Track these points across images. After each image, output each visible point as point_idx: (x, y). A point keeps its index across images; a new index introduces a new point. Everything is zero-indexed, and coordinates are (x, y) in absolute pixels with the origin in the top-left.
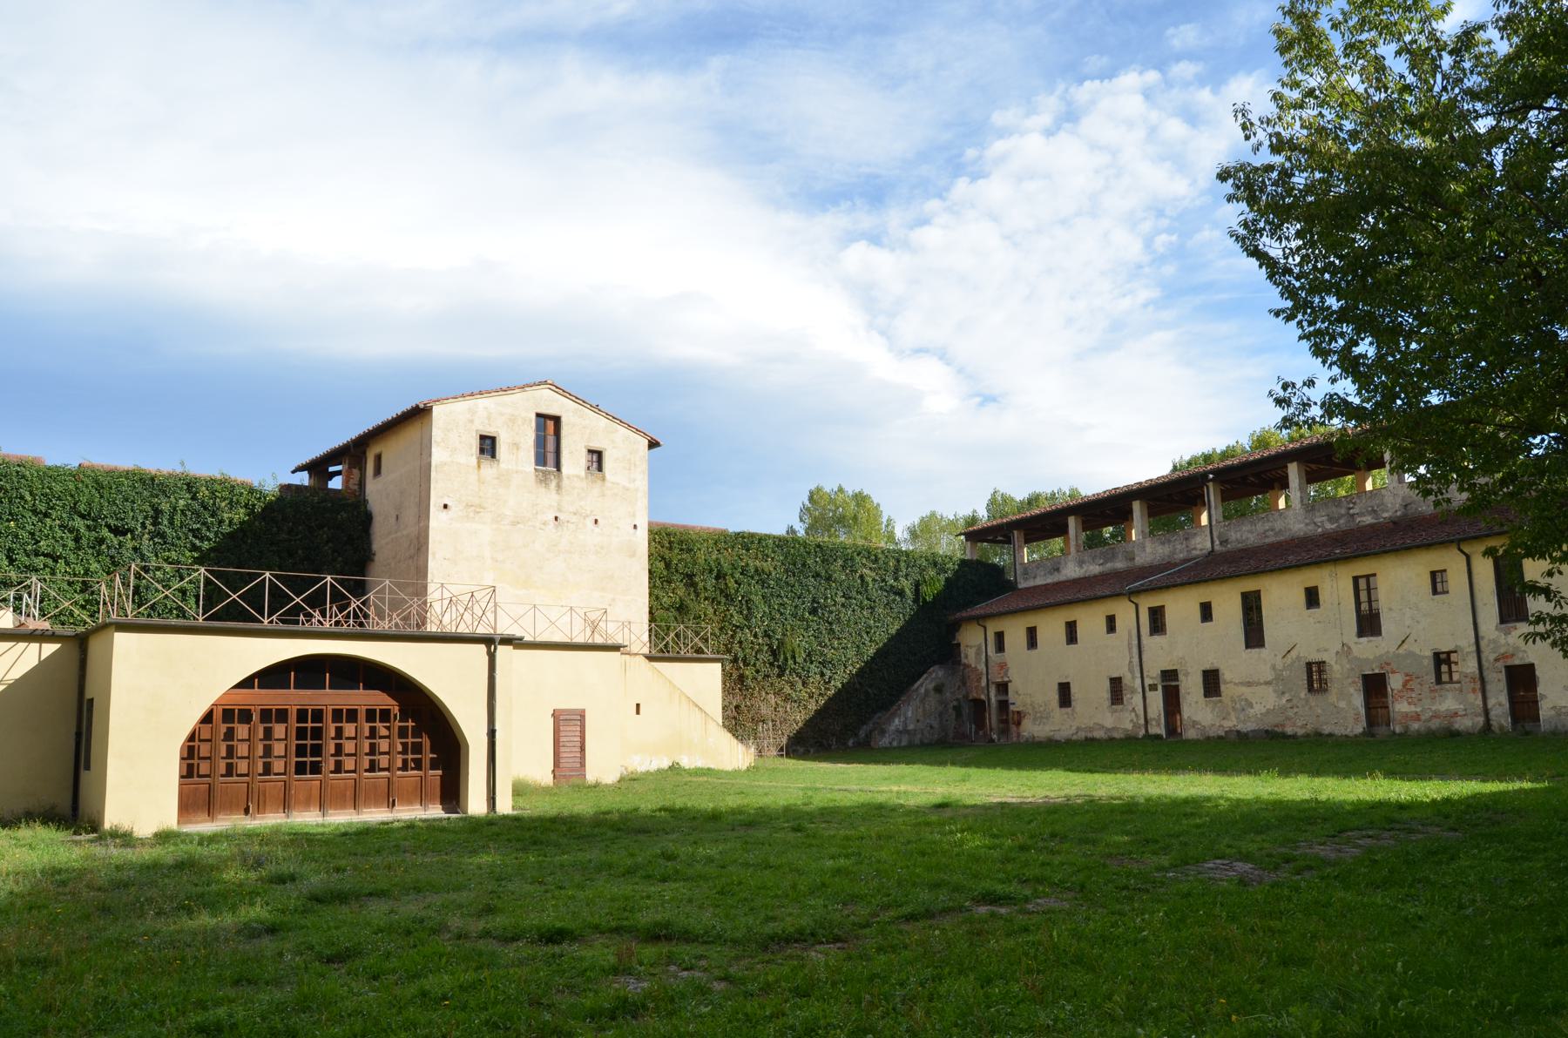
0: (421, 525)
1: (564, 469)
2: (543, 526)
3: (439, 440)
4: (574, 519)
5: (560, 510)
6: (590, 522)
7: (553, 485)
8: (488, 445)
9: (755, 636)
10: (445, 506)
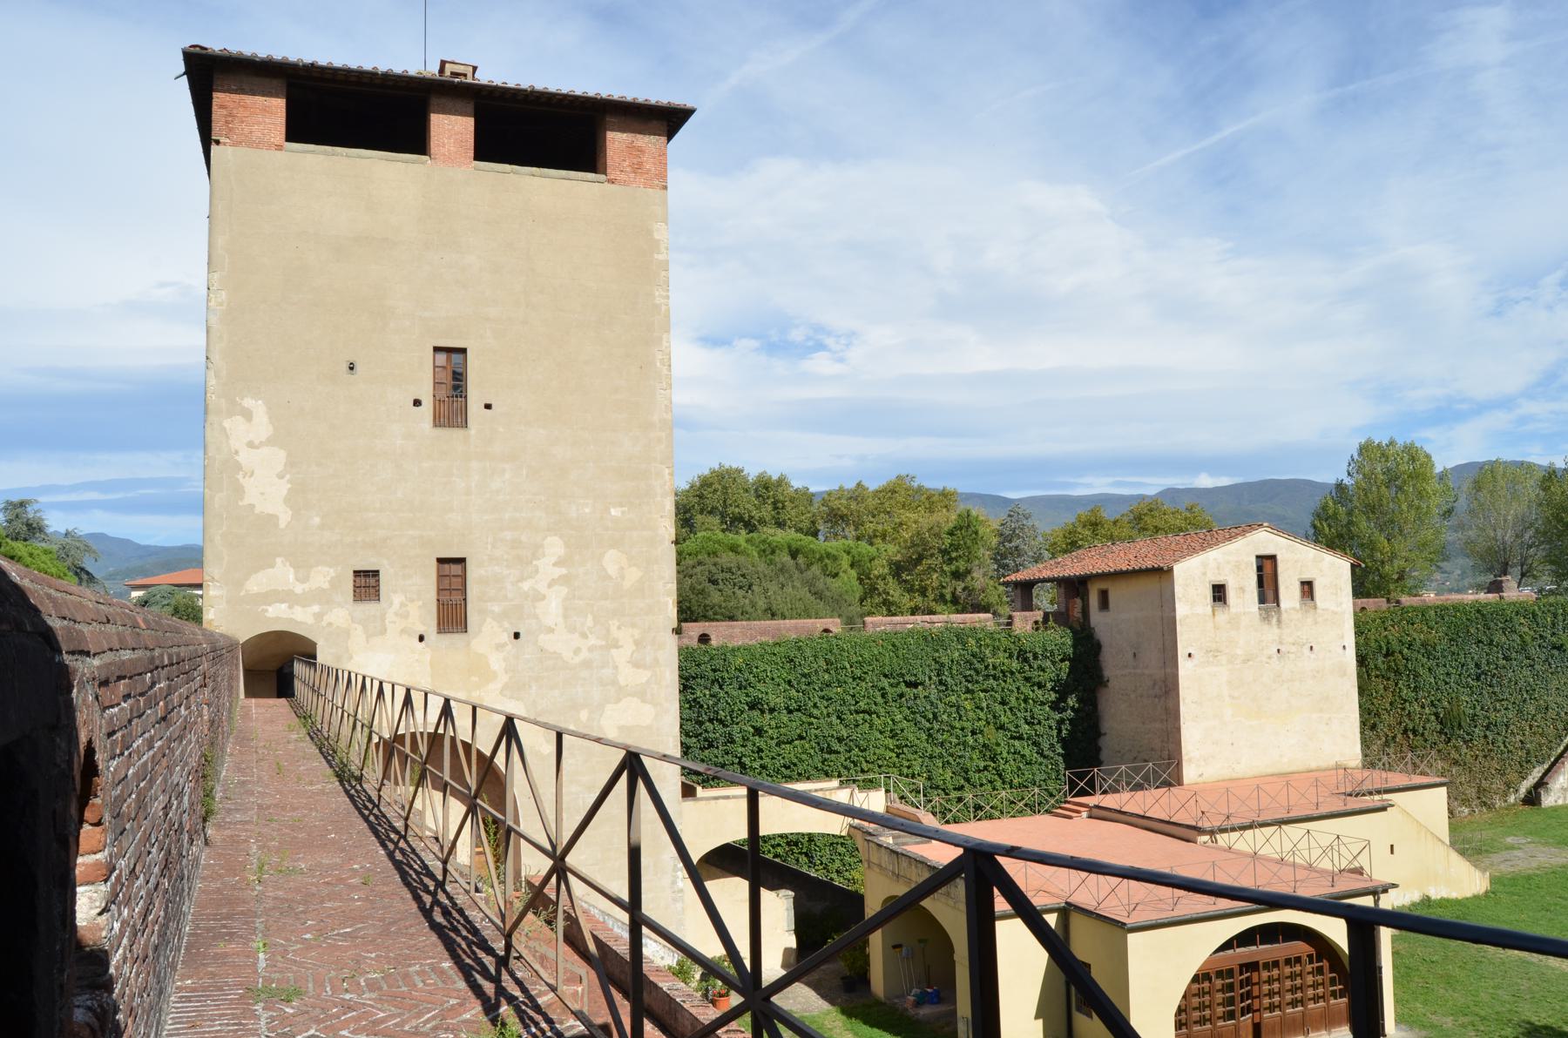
0: (1168, 670)
1: (1283, 605)
2: (1268, 660)
3: (1180, 596)
4: (1293, 649)
5: (1281, 643)
6: (1306, 650)
7: (1274, 620)
8: (1219, 593)
9: (1423, 707)
10: (1190, 655)
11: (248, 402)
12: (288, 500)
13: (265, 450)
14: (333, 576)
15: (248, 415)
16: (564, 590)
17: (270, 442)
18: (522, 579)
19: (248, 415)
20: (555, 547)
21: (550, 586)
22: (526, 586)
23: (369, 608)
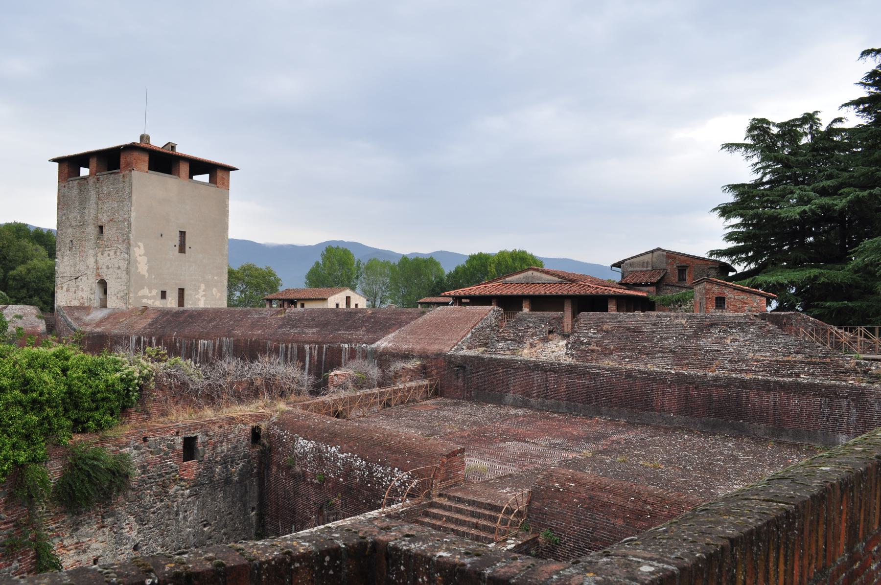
11: (139, 244)
12: (147, 271)
13: (143, 257)
14: (156, 292)
15: (139, 247)
16: (205, 298)
17: (144, 255)
18: (196, 295)
19: (139, 247)
20: (203, 286)
21: (202, 296)
22: (196, 297)
23: (164, 301)
